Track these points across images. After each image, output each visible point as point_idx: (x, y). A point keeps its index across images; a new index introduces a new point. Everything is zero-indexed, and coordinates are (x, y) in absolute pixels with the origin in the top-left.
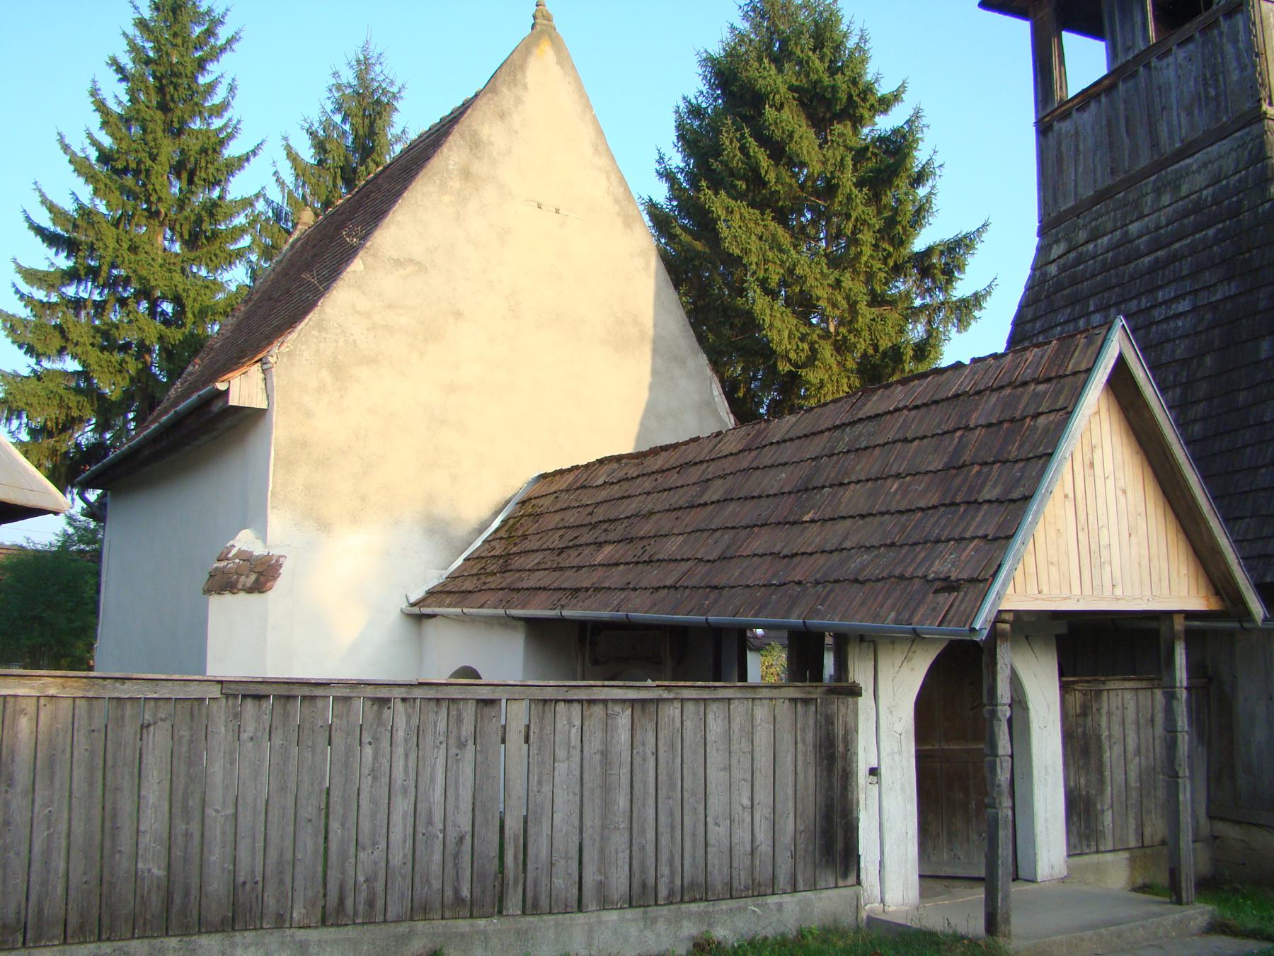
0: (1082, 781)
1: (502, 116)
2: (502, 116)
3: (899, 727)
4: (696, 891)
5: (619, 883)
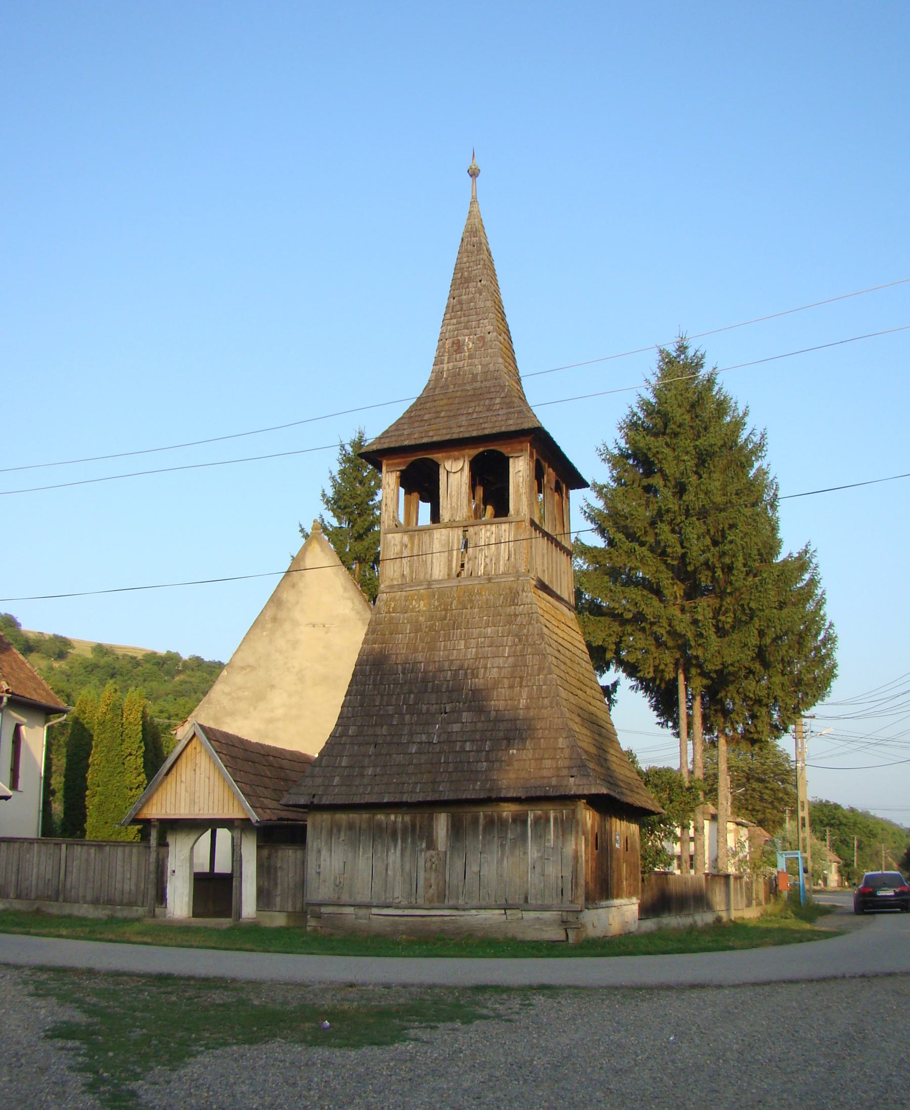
0: (266, 884)
1: (293, 586)
2: (293, 586)
3: (182, 857)
4: (110, 902)
5: (89, 897)
